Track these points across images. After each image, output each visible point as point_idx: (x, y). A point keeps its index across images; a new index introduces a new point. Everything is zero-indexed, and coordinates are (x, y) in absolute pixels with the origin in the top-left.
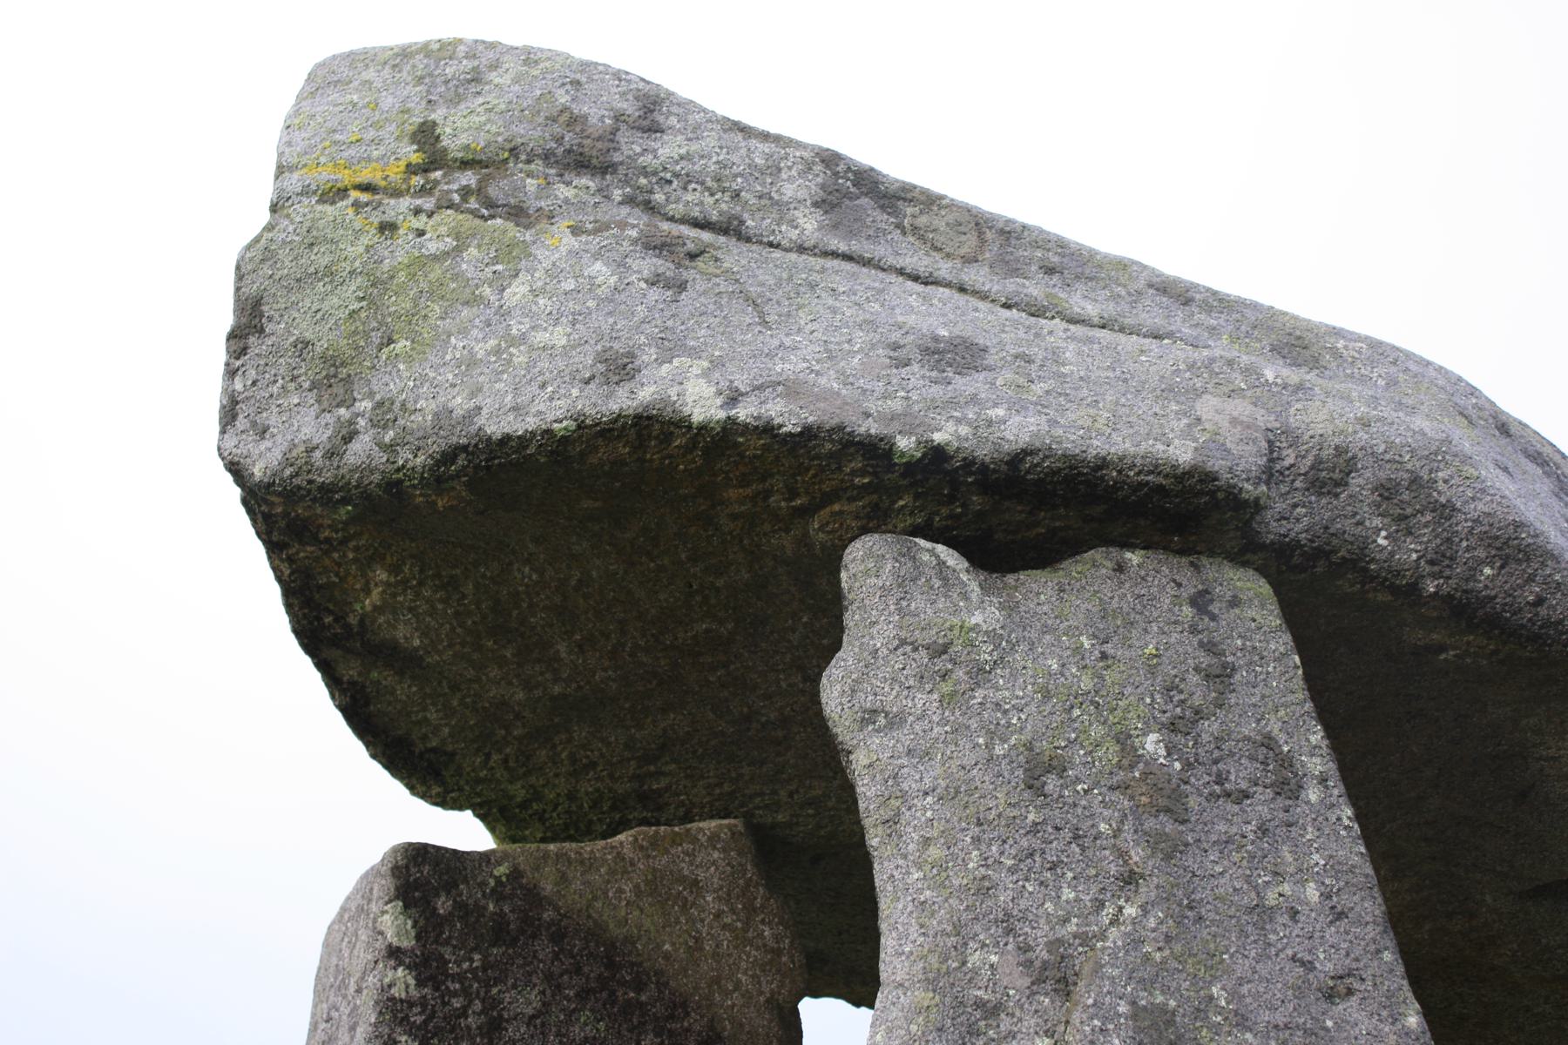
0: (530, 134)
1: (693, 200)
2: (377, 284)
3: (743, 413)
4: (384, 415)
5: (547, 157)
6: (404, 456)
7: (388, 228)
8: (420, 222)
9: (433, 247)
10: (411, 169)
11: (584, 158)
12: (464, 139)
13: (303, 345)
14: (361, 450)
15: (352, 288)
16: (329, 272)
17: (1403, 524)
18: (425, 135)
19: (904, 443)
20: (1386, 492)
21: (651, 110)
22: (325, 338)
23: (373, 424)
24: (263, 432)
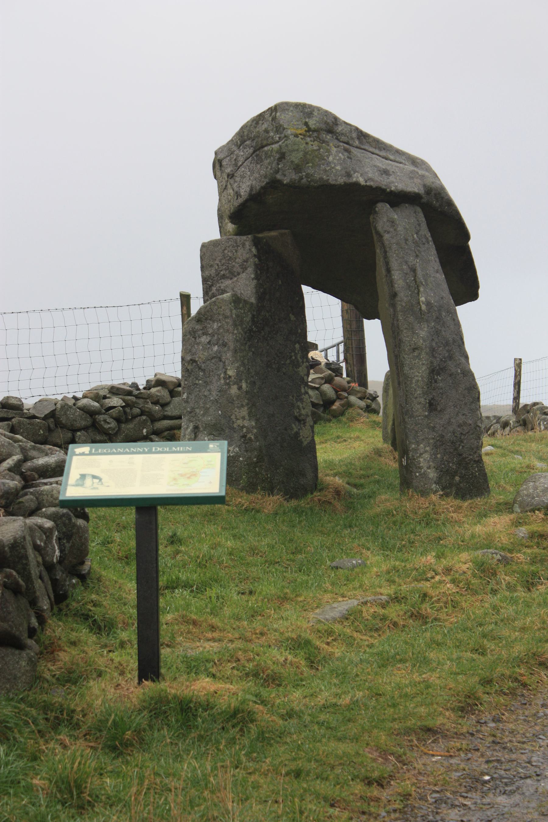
0: (323, 126)
1: (343, 138)
2: (306, 153)
3: (368, 184)
4: (308, 176)
5: (326, 131)
6: (312, 183)
7: (307, 143)
8: (312, 143)
9: (315, 148)
10: (306, 131)
11: (330, 131)
12: (314, 126)
13: (292, 162)
14: (304, 181)
15: (301, 153)
16: (297, 150)
17: (437, 200)
18: (306, 124)
19: (388, 190)
20: (435, 194)
21: (336, 120)
22: (296, 161)
23: (306, 177)
24: (285, 175)
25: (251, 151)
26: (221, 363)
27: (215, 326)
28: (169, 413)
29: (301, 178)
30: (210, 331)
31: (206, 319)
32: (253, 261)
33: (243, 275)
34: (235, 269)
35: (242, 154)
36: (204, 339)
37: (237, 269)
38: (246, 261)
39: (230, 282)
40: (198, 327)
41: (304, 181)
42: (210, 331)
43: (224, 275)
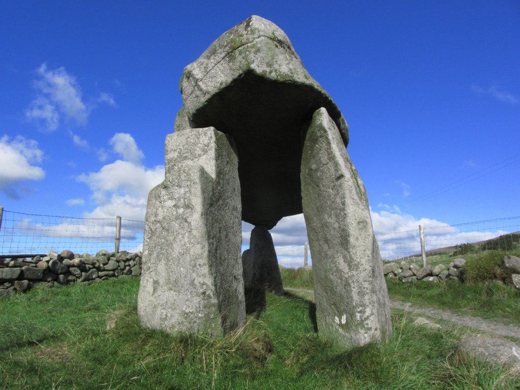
14: (273, 74)
25: (223, 55)
26: (186, 224)
27: (182, 191)
28: (106, 268)
29: (271, 72)
30: (177, 196)
31: (173, 185)
32: (213, 145)
33: (204, 157)
34: (196, 152)
35: (212, 61)
36: (170, 203)
37: (198, 151)
38: (208, 145)
39: (192, 162)
40: (163, 192)
41: (273, 74)
42: (177, 196)
43: (186, 157)
